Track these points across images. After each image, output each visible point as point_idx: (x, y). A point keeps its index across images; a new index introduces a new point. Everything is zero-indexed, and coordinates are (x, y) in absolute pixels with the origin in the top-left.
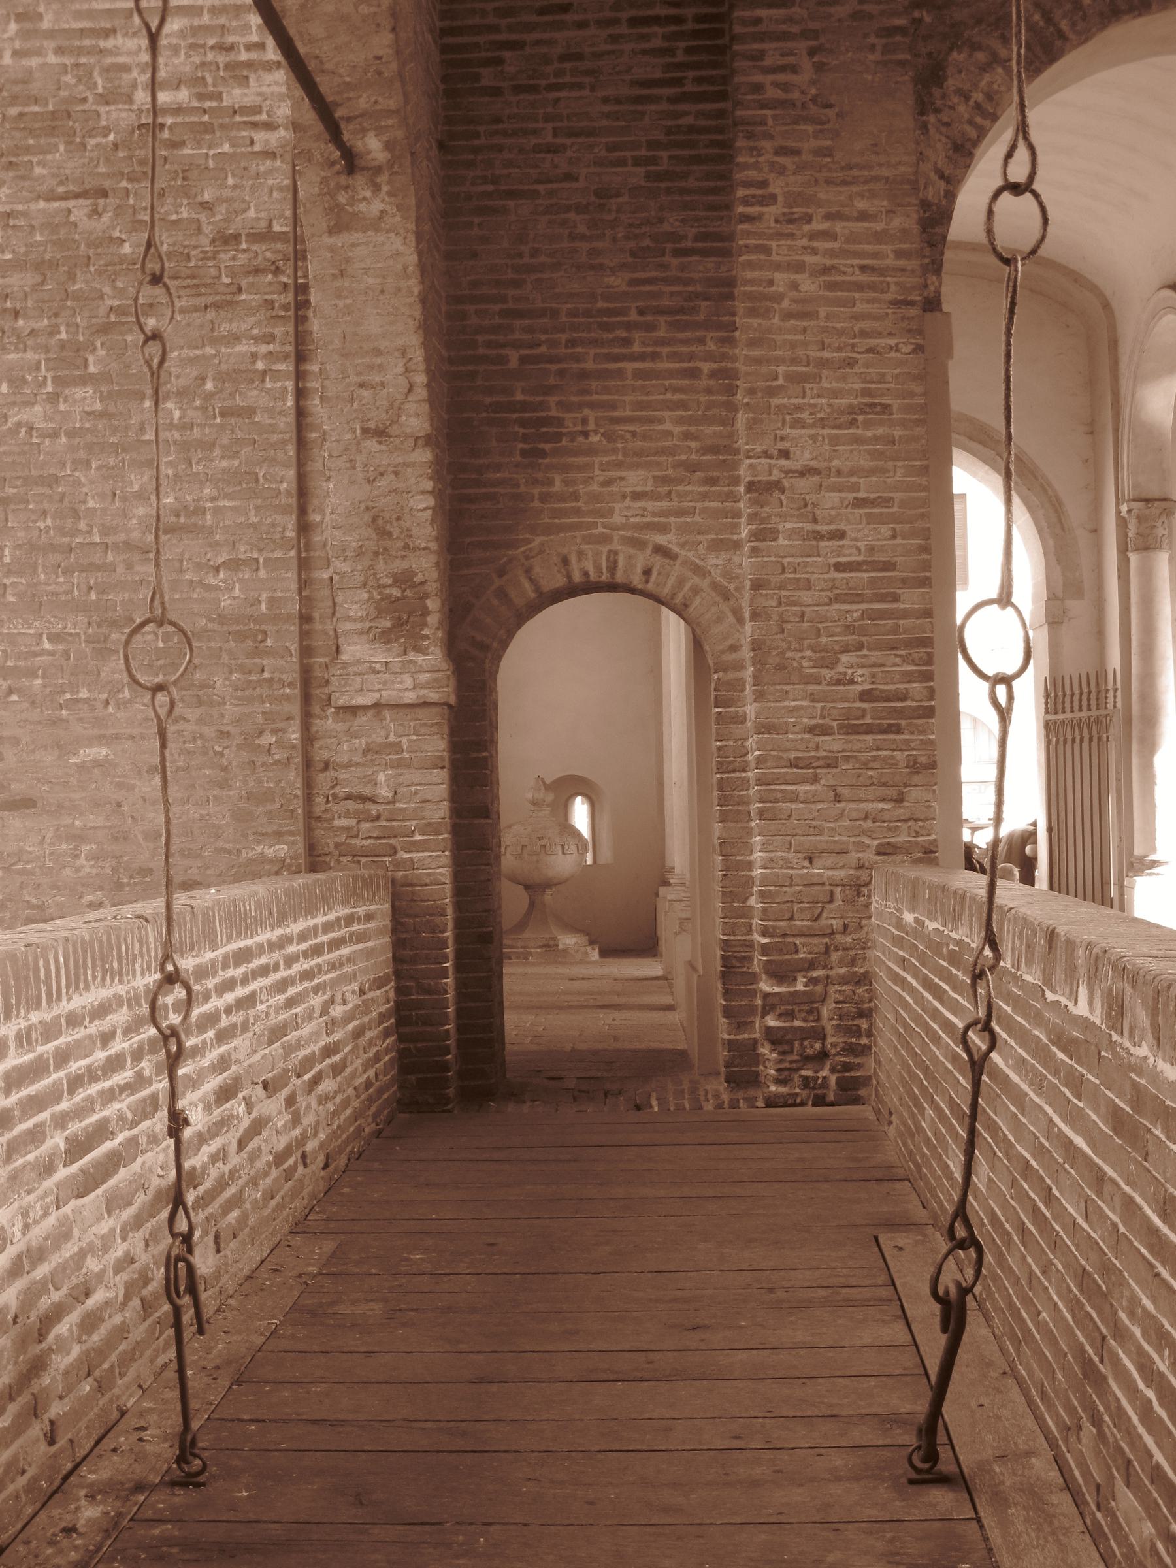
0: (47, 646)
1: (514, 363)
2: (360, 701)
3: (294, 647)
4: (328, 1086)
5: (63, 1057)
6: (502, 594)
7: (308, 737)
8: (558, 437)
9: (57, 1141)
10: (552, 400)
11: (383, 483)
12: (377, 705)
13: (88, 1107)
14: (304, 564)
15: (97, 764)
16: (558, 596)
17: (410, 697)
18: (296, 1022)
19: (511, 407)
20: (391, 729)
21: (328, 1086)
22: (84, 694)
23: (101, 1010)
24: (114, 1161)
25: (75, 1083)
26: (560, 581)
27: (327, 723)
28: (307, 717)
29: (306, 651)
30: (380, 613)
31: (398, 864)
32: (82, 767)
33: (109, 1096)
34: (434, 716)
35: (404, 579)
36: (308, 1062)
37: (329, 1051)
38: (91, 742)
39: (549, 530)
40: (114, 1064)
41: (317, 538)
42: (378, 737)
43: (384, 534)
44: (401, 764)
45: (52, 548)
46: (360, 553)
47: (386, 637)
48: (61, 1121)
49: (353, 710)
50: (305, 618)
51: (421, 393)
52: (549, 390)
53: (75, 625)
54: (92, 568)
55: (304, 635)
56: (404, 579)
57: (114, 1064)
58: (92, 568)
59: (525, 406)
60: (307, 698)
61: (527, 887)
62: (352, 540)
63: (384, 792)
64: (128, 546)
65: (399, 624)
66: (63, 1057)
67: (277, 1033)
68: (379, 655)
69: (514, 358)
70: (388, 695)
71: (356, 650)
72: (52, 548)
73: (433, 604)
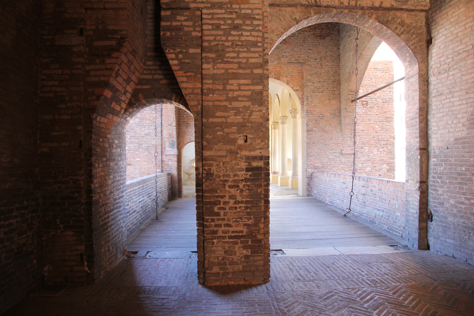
0: (133, 147)
1: (185, 117)
2: (168, 154)
3: (160, 148)
4: (165, 194)
5: (147, 187)
6: (183, 142)
7: (162, 158)
8: (190, 125)
9: (147, 193)
10: (189, 121)
11: (170, 131)
12: (169, 155)
13: (148, 191)
14: (162, 139)
15: (138, 160)
16: (189, 142)
17: (173, 154)
18: (162, 187)
19: (185, 122)
20: (171, 157)
21: (165, 194)
22: (137, 153)
23: (150, 184)
24: (150, 196)
25: (148, 189)
26: (190, 141)
27: (164, 156)
28: (162, 156)
29: (162, 149)
30: (170, 144)
31: (172, 172)
32: (137, 161)
33: (150, 191)
34: (176, 156)
35: (173, 141)
36: (163, 191)
37: (165, 191)
38: (138, 158)
39: (189, 135)
40: (150, 188)
41: (163, 136)
42: (169, 158)
43: (170, 136)
44: (172, 161)
45: (134, 136)
46: (168, 138)
47: (171, 147)
48: (148, 192)
49: (167, 155)
50: (162, 145)
51: (175, 121)
52: (189, 120)
53: (136, 145)
54: (138, 139)
55: (162, 147)
56: (173, 141)
57: (150, 188)
58: (138, 139)
59: (186, 122)
60: (162, 154)
61: (188, 175)
62: (167, 137)
63: (170, 164)
64: (142, 137)
65: (172, 146)
66: (147, 187)
67: (161, 188)
68: (170, 149)
69: (185, 116)
70: (171, 154)
71: (167, 149)
72: (134, 136)
73: (176, 144)
